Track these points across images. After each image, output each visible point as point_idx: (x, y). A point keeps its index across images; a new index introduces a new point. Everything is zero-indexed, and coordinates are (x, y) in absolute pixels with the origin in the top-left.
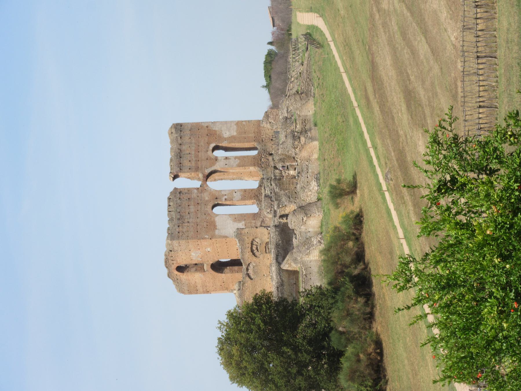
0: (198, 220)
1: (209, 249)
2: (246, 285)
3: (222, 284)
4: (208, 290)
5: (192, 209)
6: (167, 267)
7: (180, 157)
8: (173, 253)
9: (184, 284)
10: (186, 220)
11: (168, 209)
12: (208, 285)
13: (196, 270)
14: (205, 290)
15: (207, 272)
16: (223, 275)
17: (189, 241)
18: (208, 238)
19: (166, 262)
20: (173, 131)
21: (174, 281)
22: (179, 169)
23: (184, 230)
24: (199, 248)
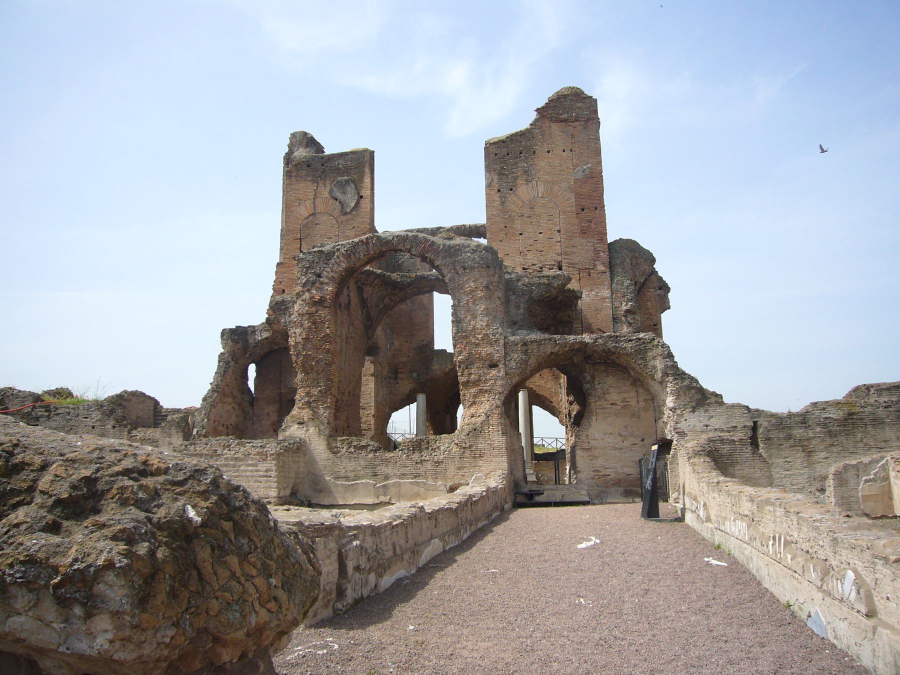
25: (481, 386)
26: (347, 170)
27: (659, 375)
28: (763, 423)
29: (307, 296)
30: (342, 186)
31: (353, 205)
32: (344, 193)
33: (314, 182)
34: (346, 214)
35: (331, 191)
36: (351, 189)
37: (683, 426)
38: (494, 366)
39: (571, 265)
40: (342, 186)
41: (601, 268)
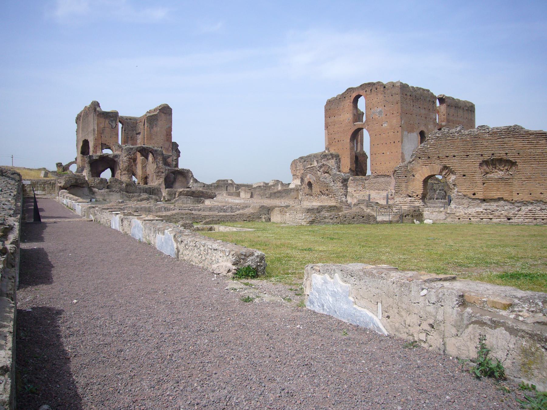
0: (414, 116)
1: (385, 125)
2: (541, 142)
3: (336, 139)
4: (329, 127)
5: (423, 112)
6: (361, 86)
7: (455, 107)
8: (382, 89)
9: (339, 104)
10: (414, 104)
11: (422, 89)
12: (336, 126)
13: (354, 115)
14: (330, 124)
15: (352, 125)
16: (349, 141)
17: (399, 104)
18: (401, 124)
19: (369, 84)
20: (471, 105)
21: (343, 94)
22: (449, 104)
23: (407, 100)
24: (388, 114)
25: (161, 177)
26: (112, 117)
27: (190, 177)
28: (205, 186)
29: (128, 156)
30: (112, 121)
31: (114, 126)
32: (112, 123)
33: (104, 118)
34: (113, 128)
35: (109, 122)
36: (114, 122)
37: (194, 185)
38: (163, 173)
39: (164, 148)
40: (112, 121)
41: (170, 149)
